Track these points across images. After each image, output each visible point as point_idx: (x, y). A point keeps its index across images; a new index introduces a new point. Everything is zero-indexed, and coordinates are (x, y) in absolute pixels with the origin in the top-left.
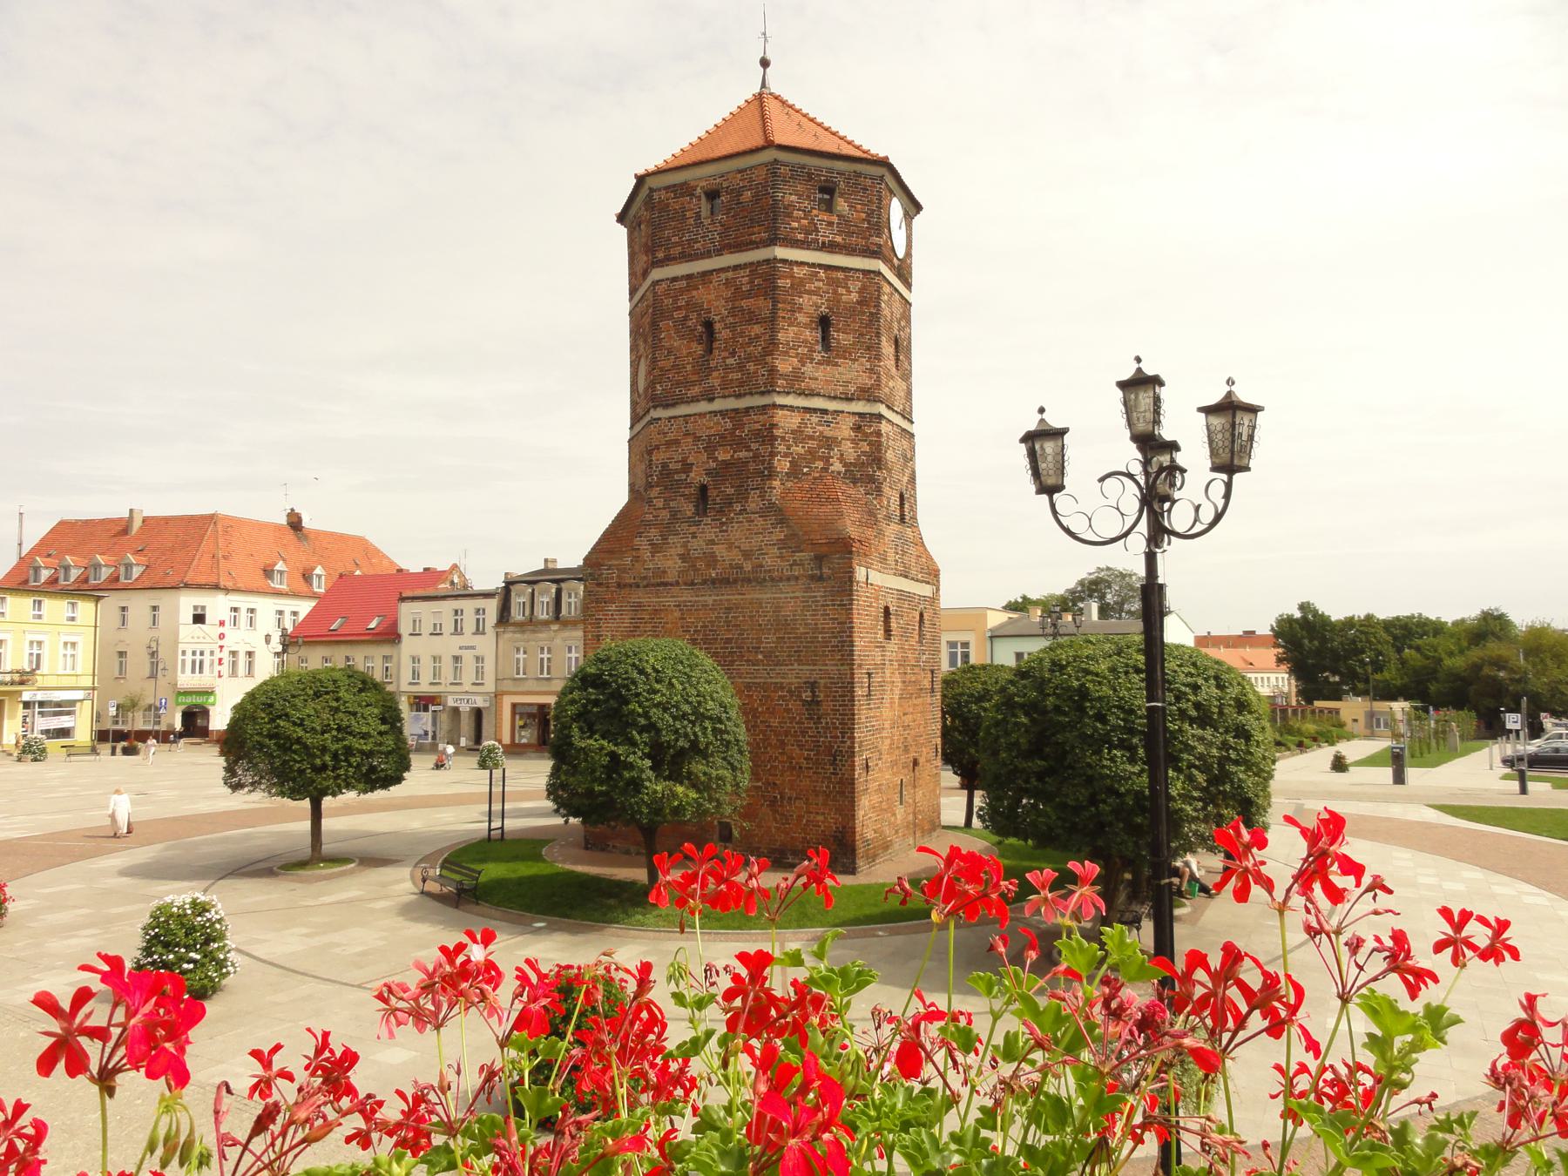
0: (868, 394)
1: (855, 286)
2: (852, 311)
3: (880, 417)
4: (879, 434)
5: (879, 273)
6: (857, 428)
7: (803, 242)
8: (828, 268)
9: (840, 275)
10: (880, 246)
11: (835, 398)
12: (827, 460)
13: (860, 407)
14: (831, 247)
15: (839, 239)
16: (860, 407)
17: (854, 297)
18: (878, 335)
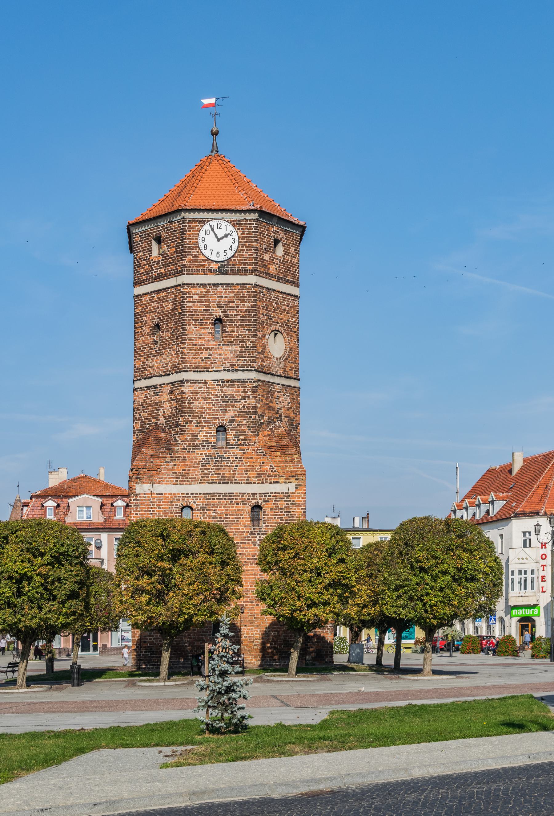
0: (177, 369)
1: (170, 299)
2: (170, 316)
3: (182, 382)
4: (182, 393)
5: (183, 285)
6: (171, 392)
7: (148, 280)
8: (158, 291)
9: (164, 294)
10: (184, 266)
11: (161, 376)
12: (157, 417)
13: (173, 378)
14: (160, 278)
15: (162, 271)
16: (173, 378)
17: (171, 306)
18: (183, 327)
